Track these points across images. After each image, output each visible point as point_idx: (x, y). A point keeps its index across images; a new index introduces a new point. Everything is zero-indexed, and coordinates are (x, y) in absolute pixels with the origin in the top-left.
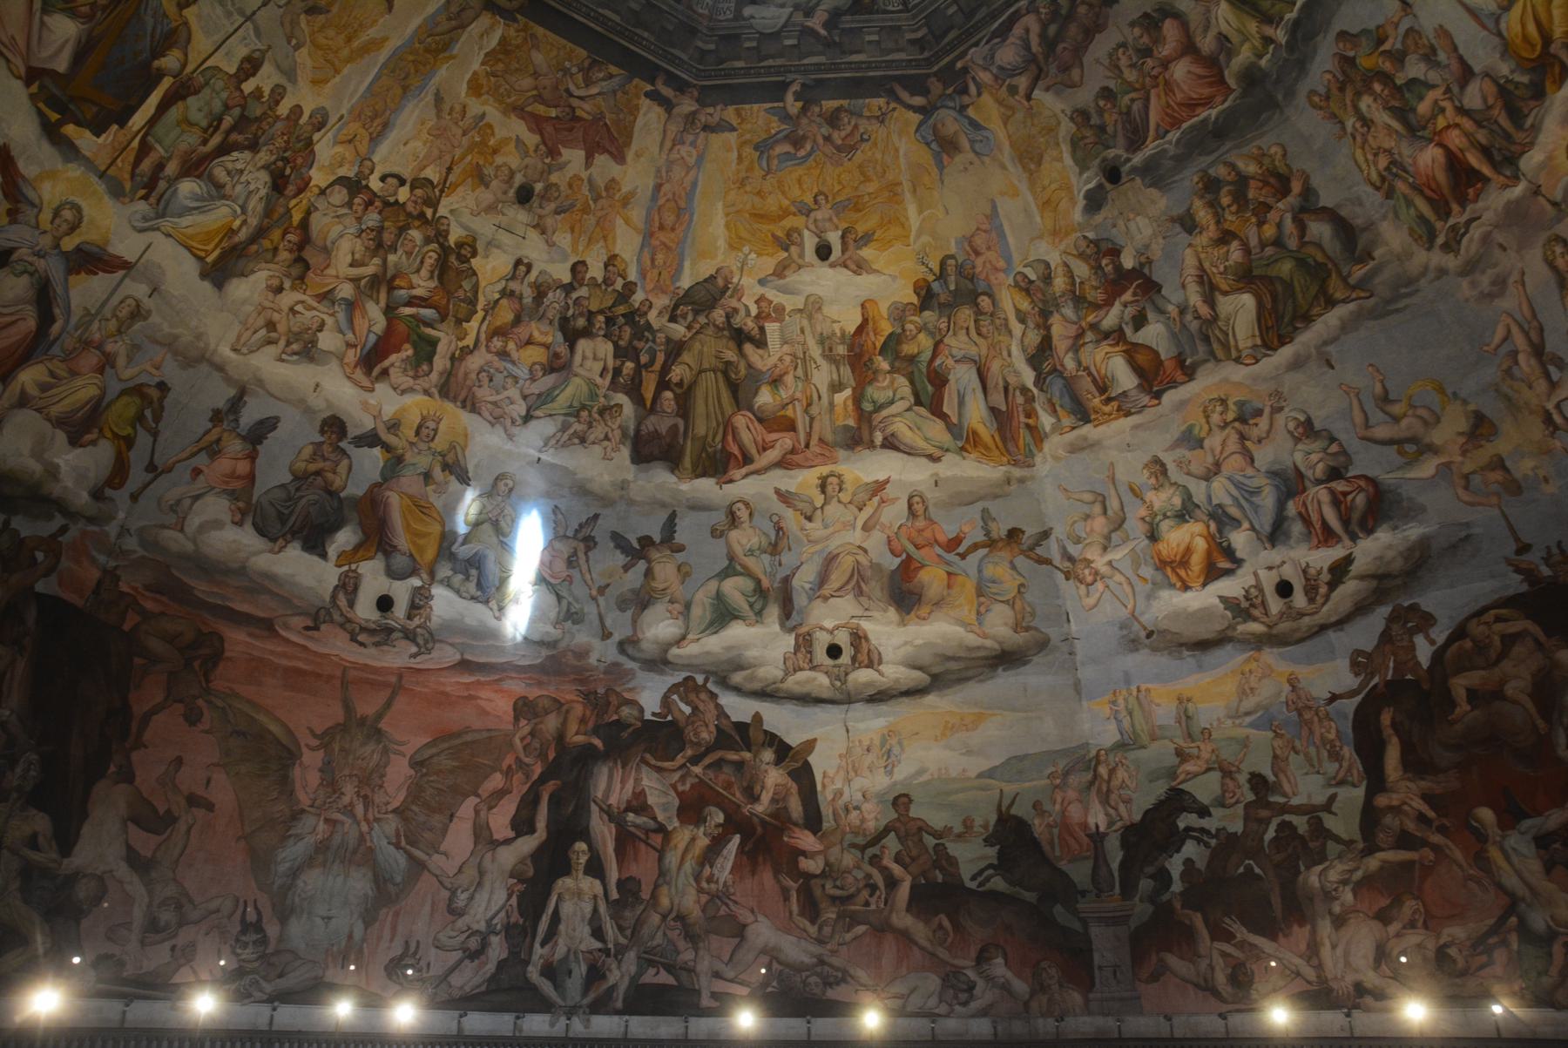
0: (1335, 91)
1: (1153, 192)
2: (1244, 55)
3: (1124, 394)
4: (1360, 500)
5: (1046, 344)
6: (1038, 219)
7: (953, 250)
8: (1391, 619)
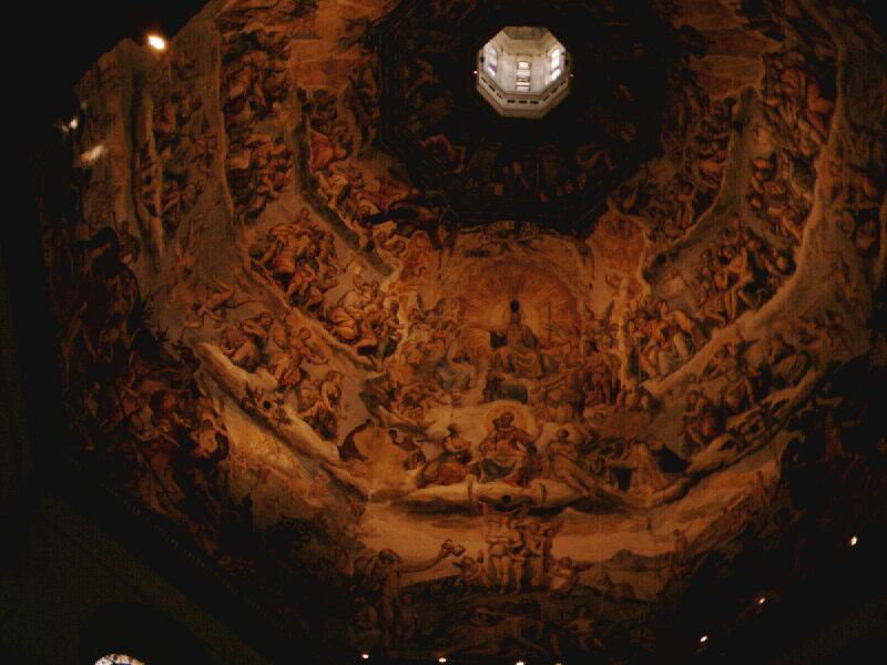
0: (309, 224)
1: (294, 127)
2: (323, 182)
3: (229, 90)
4: (173, 219)
5: (258, 47)
6: (307, 61)
7: (317, 12)
8: (136, 240)
